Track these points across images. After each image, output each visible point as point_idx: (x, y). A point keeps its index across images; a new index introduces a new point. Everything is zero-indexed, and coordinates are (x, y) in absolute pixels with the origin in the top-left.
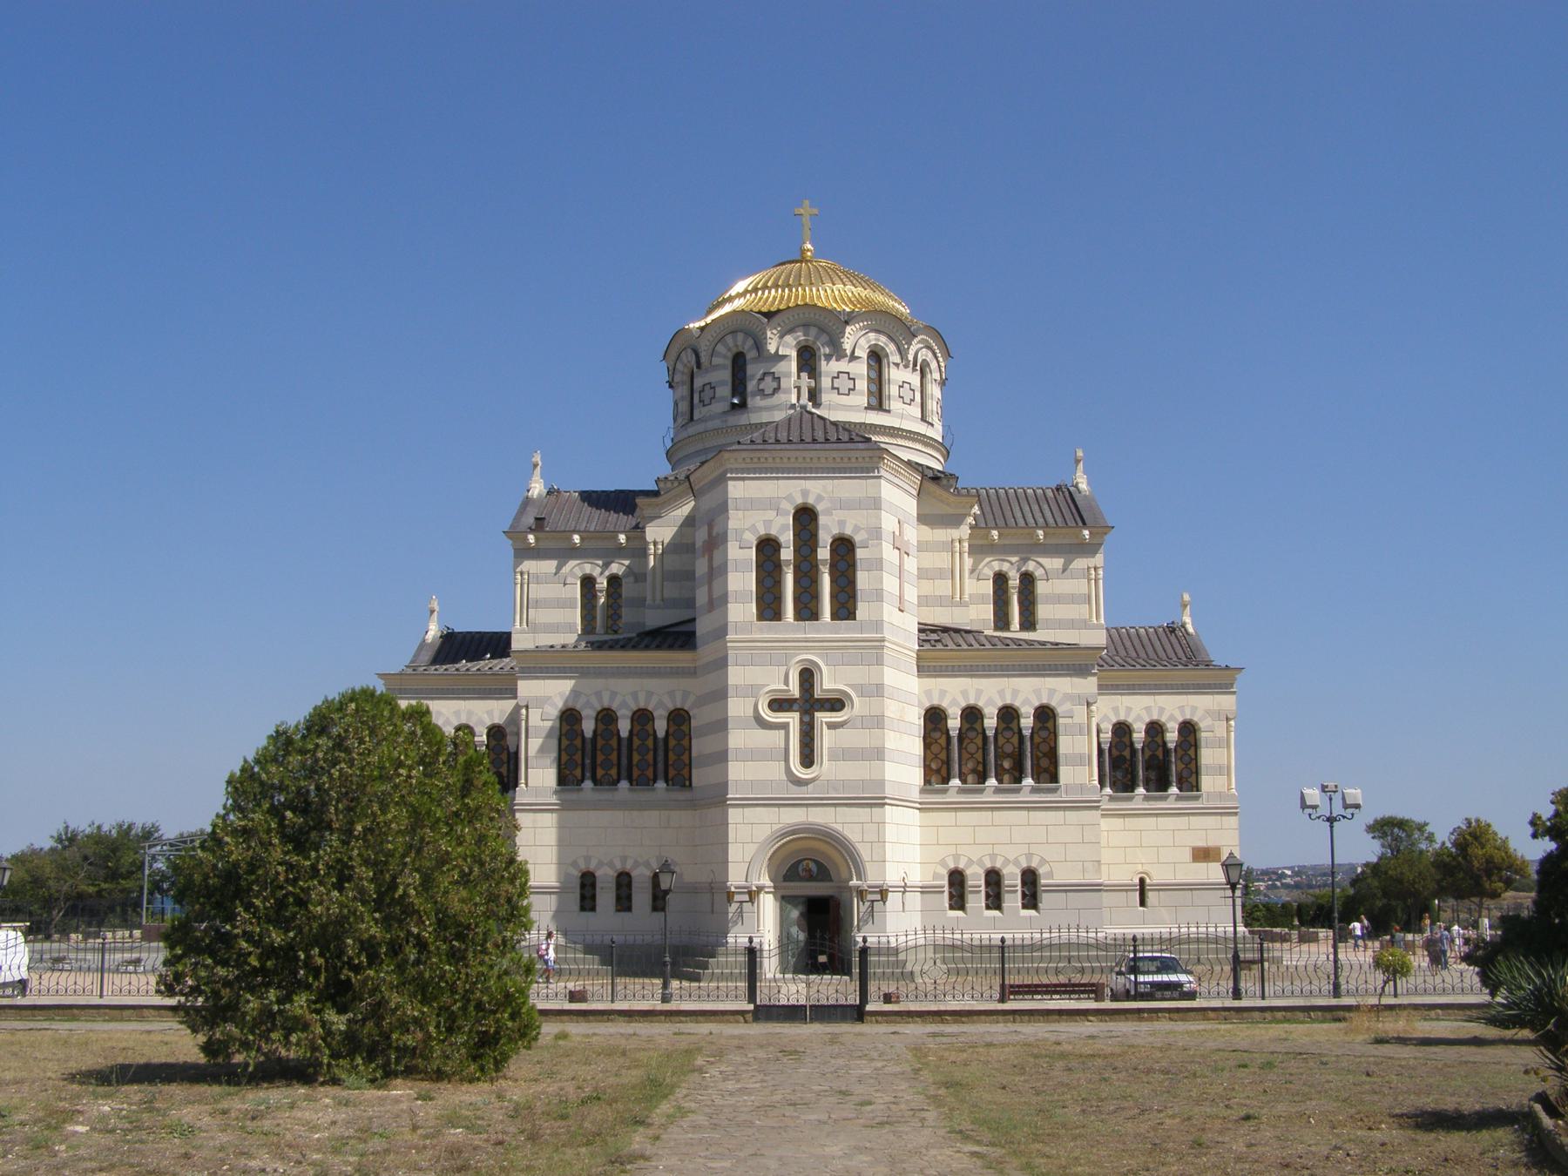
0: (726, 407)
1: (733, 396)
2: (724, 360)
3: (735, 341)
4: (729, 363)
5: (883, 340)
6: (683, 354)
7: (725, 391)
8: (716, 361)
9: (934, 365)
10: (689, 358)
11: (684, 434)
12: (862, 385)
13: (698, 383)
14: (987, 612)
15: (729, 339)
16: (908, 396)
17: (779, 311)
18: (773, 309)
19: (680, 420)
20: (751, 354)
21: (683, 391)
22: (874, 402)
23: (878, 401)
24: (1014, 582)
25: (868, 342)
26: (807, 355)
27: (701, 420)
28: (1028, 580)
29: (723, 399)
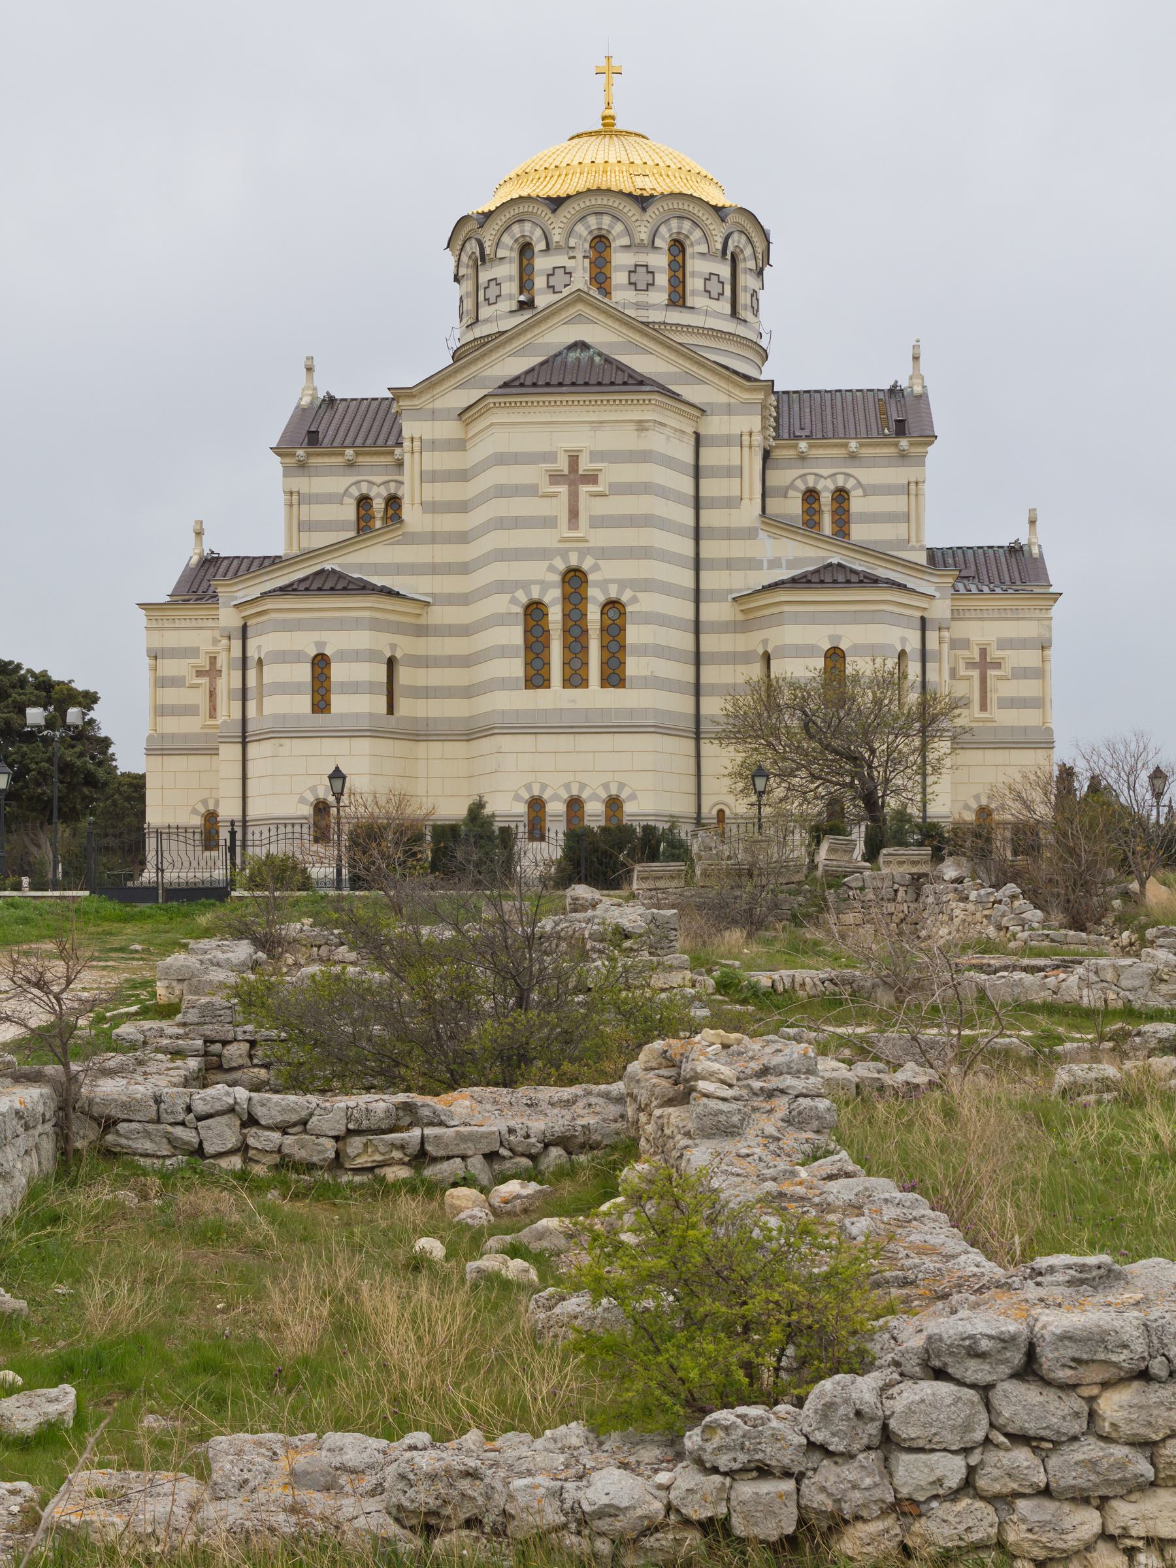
0: (514, 306)
1: (521, 293)
2: (508, 250)
3: (522, 231)
4: (515, 255)
5: (687, 225)
6: (467, 246)
7: (511, 288)
8: (501, 253)
9: (748, 251)
10: (473, 247)
11: (469, 337)
12: (662, 279)
13: (484, 276)
15: (516, 229)
16: (714, 287)
17: (569, 197)
18: (562, 194)
19: (465, 320)
20: (540, 246)
21: (468, 285)
22: (675, 298)
23: (678, 299)
24: (826, 498)
25: (670, 230)
26: (600, 247)
27: (487, 321)
28: (841, 495)
29: (511, 297)
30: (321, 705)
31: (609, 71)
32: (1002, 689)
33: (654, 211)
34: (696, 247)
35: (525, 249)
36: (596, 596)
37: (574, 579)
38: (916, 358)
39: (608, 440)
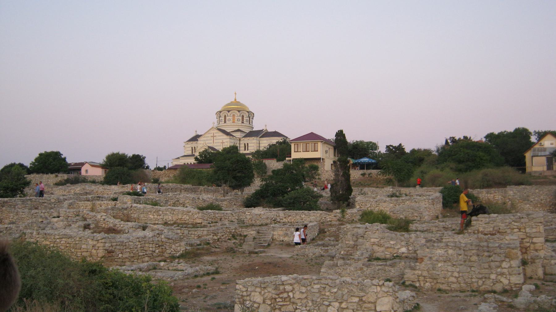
7: (218, 122)
14: (243, 148)
16: (239, 120)
23: (234, 122)
28: (248, 144)
31: (236, 94)
33: (230, 112)
38: (266, 126)
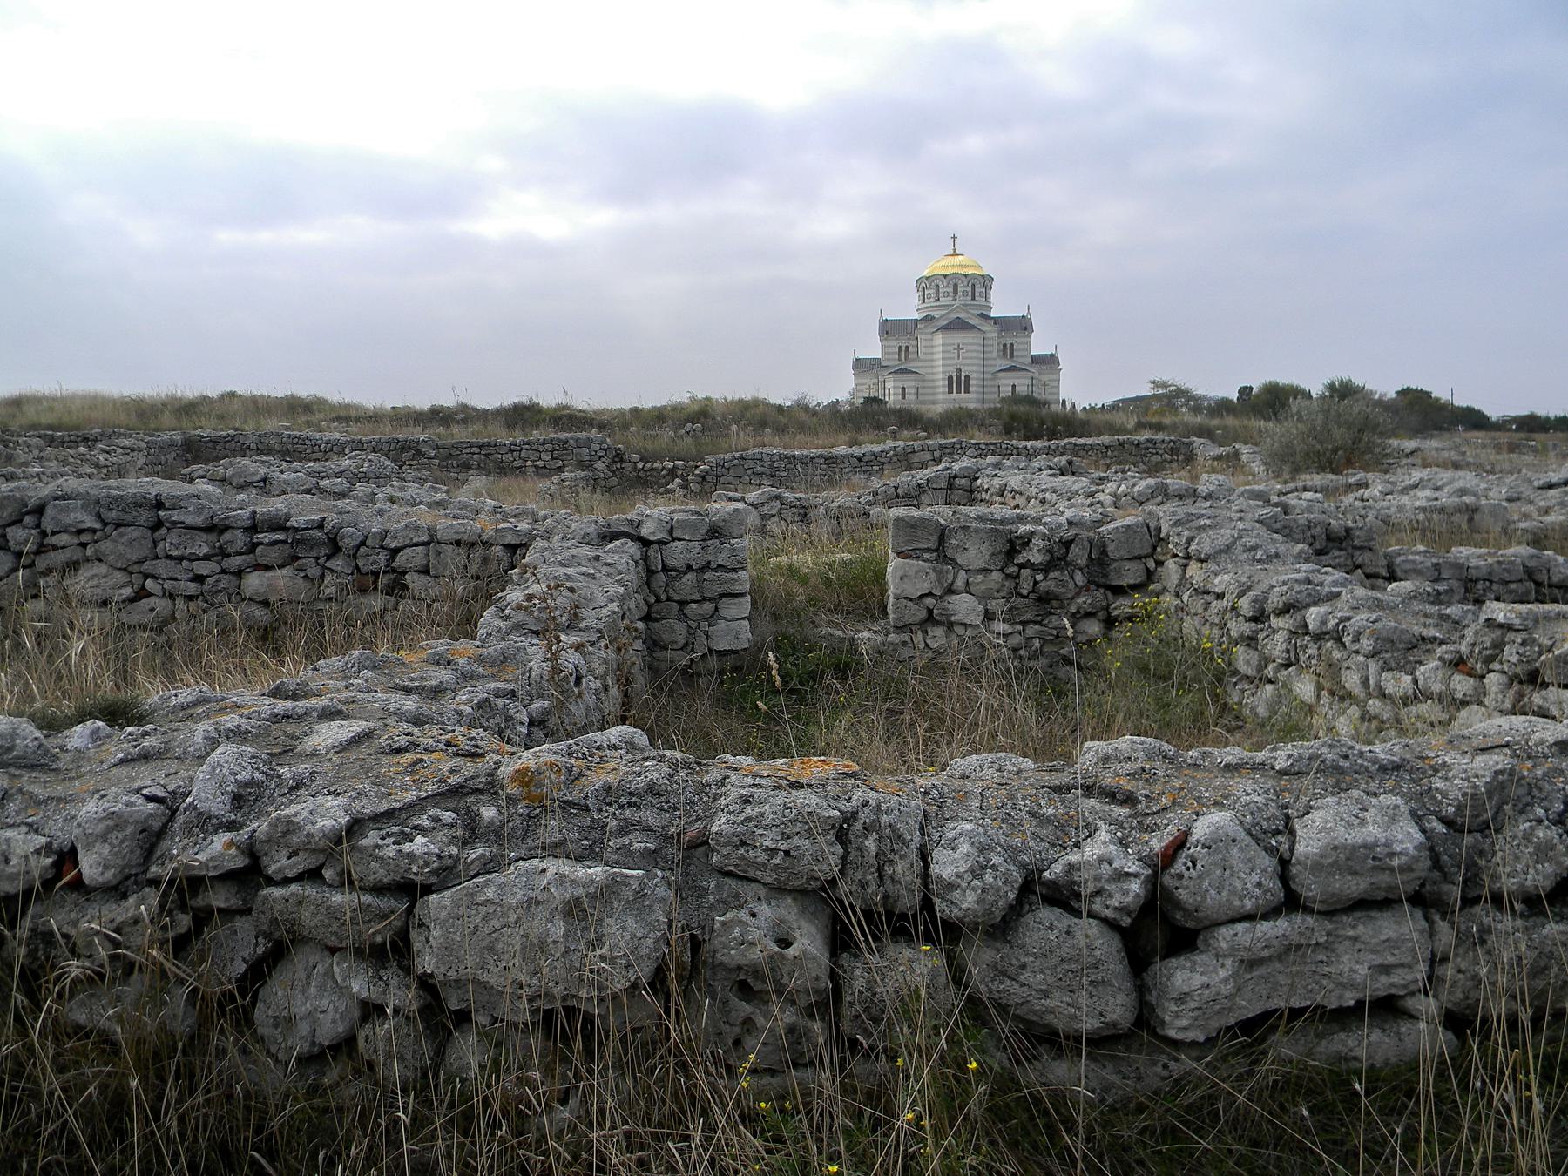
23: (973, 299)
28: (1012, 345)
30: (904, 397)
31: (954, 237)
32: (1048, 391)
34: (977, 286)
35: (937, 286)
36: (963, 374)
37: (959, 370)
39: (966, 341)
